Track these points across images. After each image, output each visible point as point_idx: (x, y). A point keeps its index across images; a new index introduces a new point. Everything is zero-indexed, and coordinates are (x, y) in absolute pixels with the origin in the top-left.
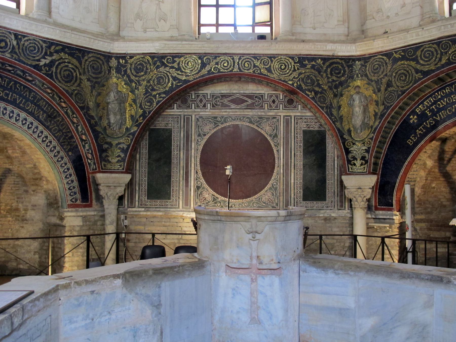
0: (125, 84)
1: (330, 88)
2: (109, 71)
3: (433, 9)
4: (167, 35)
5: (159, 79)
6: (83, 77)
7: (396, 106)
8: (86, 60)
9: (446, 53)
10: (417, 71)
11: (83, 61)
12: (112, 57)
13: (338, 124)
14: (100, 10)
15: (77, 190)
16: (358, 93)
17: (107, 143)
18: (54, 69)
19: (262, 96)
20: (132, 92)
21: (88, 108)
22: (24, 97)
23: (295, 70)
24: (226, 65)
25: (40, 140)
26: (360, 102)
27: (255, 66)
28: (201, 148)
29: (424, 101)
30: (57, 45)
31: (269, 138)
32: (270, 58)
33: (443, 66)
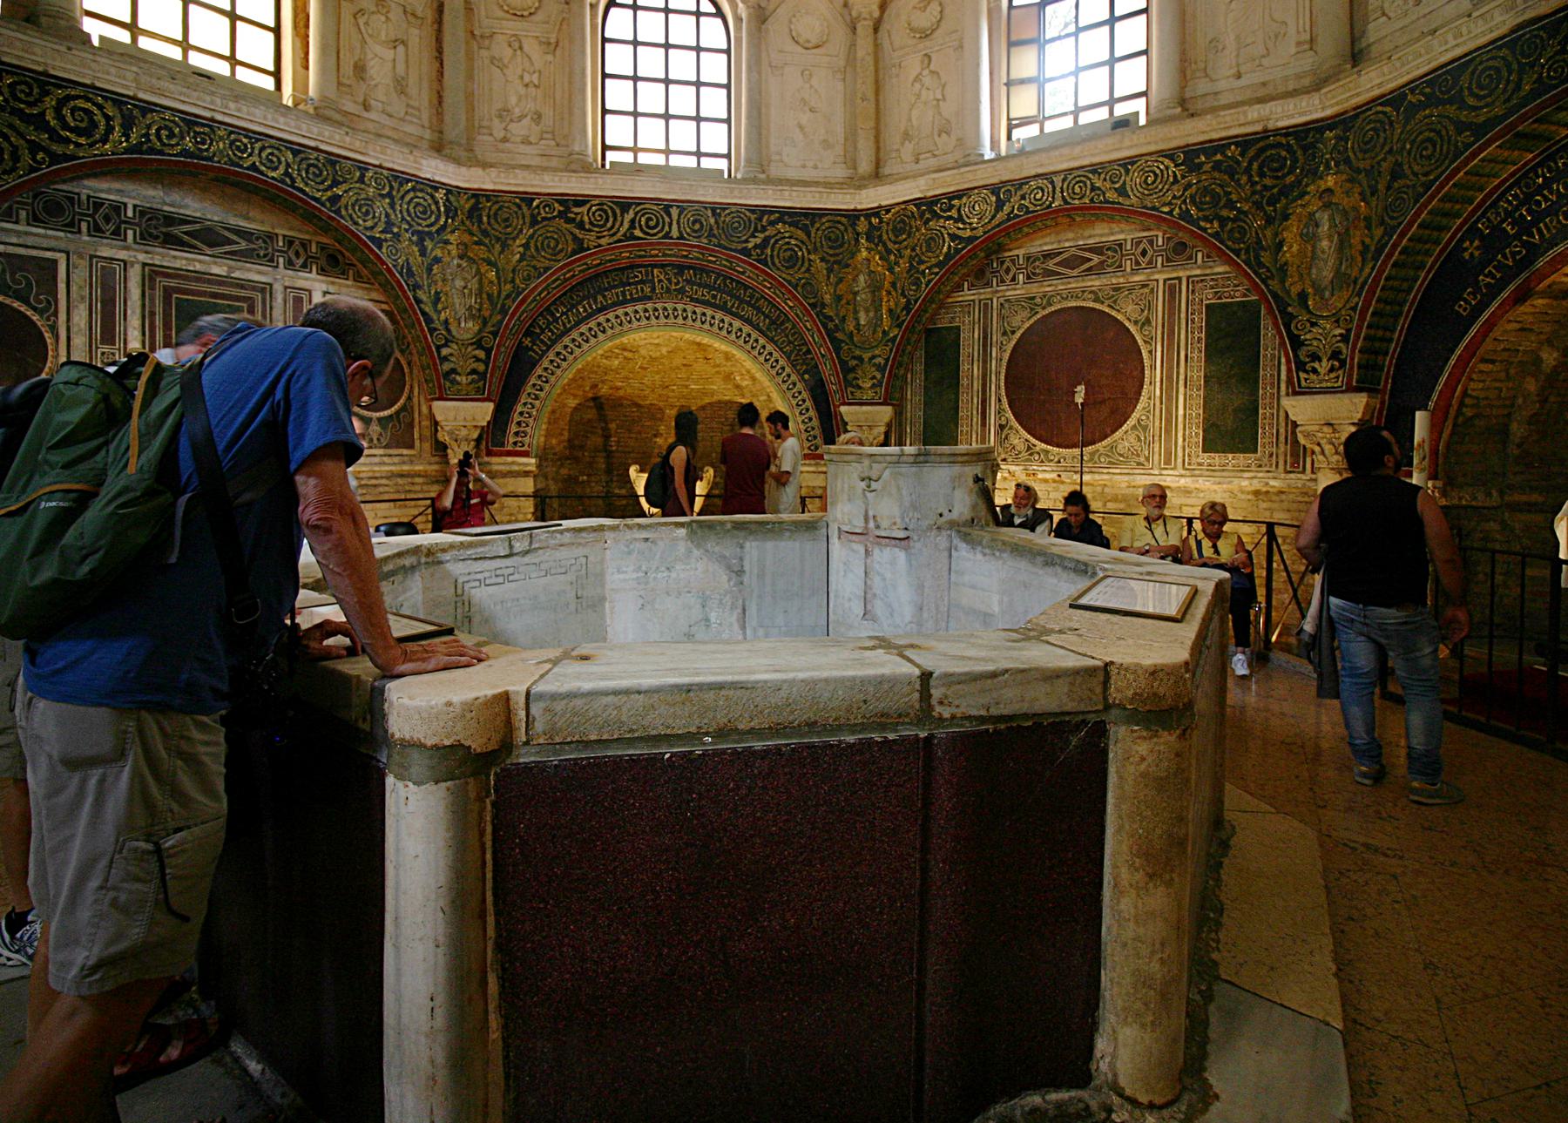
1: (1258, 206)
2: (857, 240)
5: (928, 242)
7: (1411, 224)
11: (813, 231)
12: (858, 217)
13: (1274, 284)
15: (817, 432)
16: (1327, 206)
17: (854, 358)
18: (769, 251)
19: (1120, 245)
20: (891, 270)
21: (823, 305)
22: (738, 298)
25: (762, 359)
26: (1333, 226)
28: (1007, 356)
29: (1499, 199)
30: (772, 213)
31: (1132, 329)
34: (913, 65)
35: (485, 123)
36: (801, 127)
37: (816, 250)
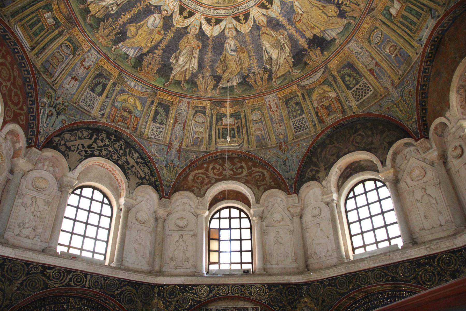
0: (162, 303)
1: (288, 303)
3: (341, 256)
4: (189, 271)
6: (138, 300)
8: (141, 289)
9: (351, 282)
10: (338, 293)
11: (139, 290)
14: (150, 256)
16: (306, 306)
18: (122, 297)
19: (247, 309)
23: (266, 293)
24: (224, 291)
27: (242, 291)
30: (125, 281)
32: (251, 286)
33: (351, 290)
34: (176, 236)
35: (12, 227)
36: (135, 250)
37: (139, 297)
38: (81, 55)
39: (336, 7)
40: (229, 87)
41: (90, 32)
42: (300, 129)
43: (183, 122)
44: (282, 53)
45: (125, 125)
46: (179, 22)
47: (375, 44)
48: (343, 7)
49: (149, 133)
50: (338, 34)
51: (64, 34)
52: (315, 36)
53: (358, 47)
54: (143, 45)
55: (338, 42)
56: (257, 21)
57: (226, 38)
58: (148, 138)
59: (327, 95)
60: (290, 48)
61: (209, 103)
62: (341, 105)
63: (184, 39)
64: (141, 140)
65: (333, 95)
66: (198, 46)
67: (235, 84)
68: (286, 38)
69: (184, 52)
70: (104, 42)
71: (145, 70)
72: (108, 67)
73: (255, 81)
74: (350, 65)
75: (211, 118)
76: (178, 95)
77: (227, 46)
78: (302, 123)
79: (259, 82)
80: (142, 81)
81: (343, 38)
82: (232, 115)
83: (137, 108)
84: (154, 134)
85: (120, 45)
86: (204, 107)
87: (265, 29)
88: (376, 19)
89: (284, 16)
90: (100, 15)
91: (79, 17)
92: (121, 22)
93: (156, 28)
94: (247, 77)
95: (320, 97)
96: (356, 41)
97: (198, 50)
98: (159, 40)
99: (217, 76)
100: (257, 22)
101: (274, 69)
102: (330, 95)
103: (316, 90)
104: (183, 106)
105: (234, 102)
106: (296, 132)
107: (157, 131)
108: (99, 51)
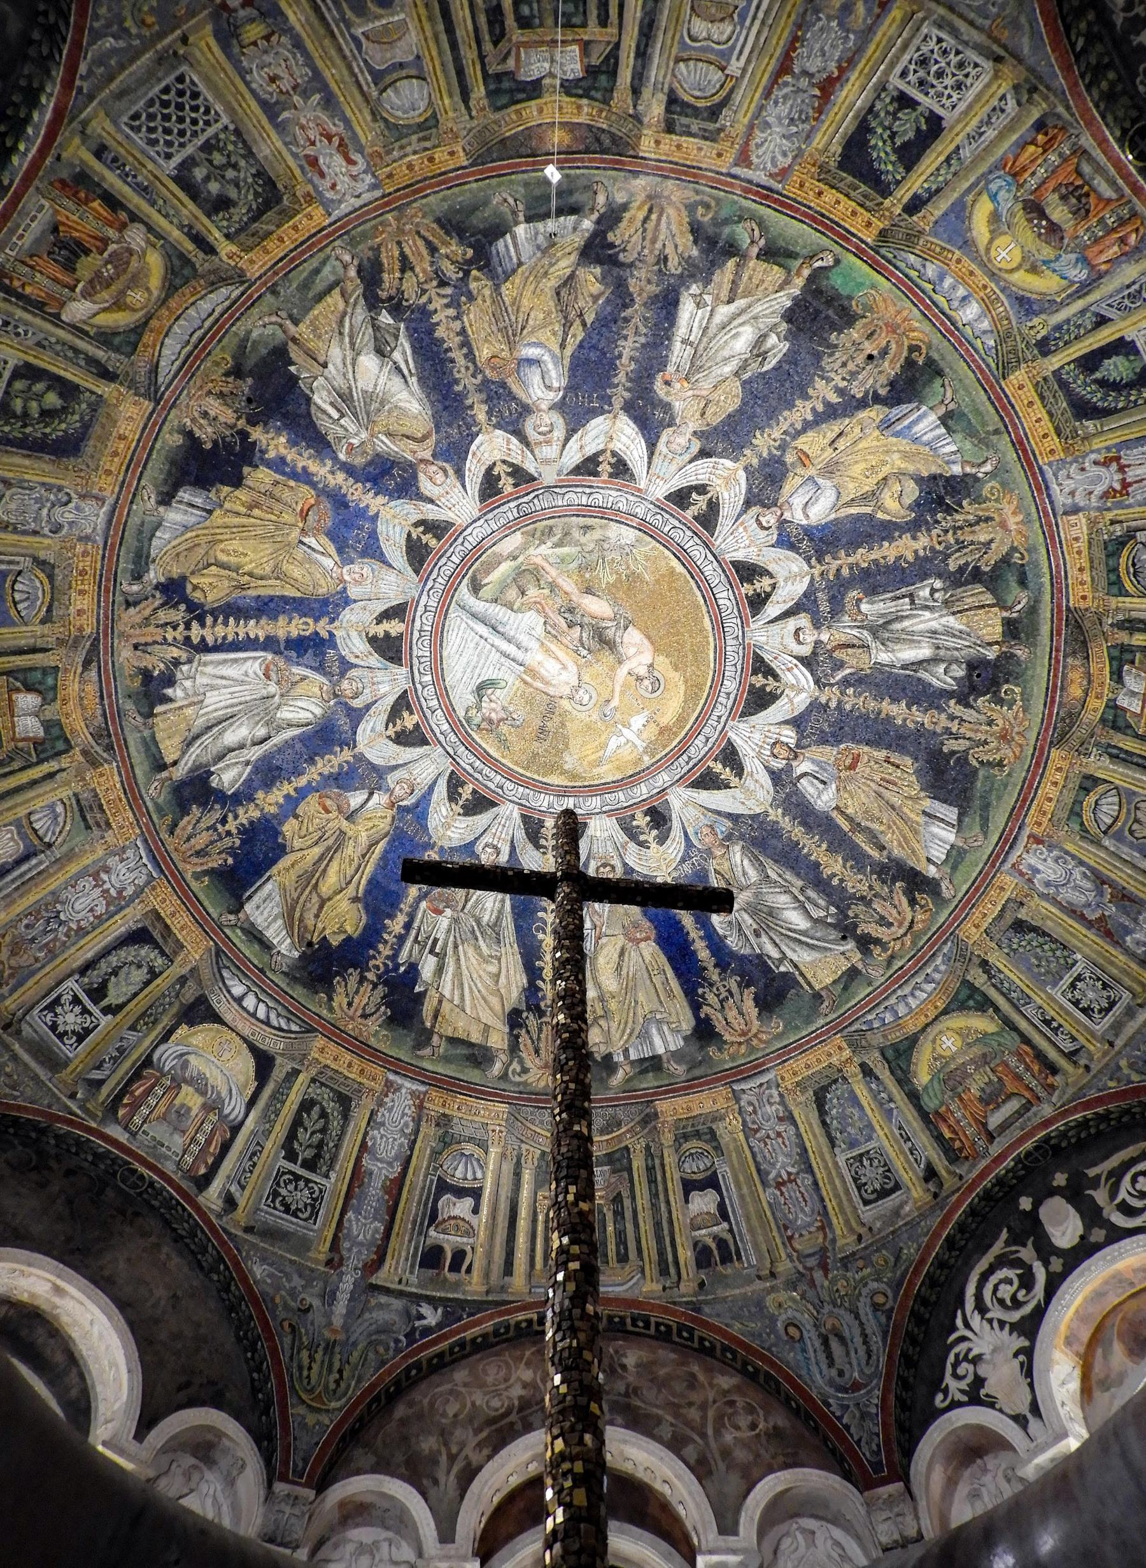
38: (1110, 515)
39: (202, 605)
40: (546, 216)
41: (1036, 564)
42: (165, 104)
43: (788, 78)
44: (339, 382)
45: (1086, 169)
46: (727, 480)
47: (20, 573)
48: (178, 614)
49: (985, 78)
50: (159, 525)
51: (1121, 617)
52: (237, 481)
53: (71, 524)
54: (873, 439)
55: (149, 498)
56: (452, 478)
57: (559, 407)
58: (998, 59)
59: (105, 295)
60: (313, 409)
61: (646, 146)
62: (20, 296)
63: (715, 416)
64: (1042, 68)
65: (78, 310)
66: (667, 383)
67: (521, 230)
68: (340, 439)
69: (728, 369)
70: (1008, 509)
71: (900, 345)
72: (1035, 420)
73: (433, 250)
74: (66, 448)
75: (639, 78)
76: (782, 204)
77: (558, 377)
78: (167, 131)
79: (414, 247)
80: (927, 307)
81: (135, 520)
82: (534, 89)
83: (995, 217)
84: (961, 65)
85: (957, 470)
86: (670, 128)
87: (421, 455)
88: (61, 642)
89: (362, 513)
90: (977, 594)
91: (1045, 629)
92: (922, 542)
93: (811, 478)
94: (469, 262)
95: (124, 278)
96: (86, 539)
97: (671, 369)
98: (810, 434)
99: (599, 261)
100: (451, 472)
101: (361, 313)
102: (88, 304)
103: (156, 293)
104: (772, 148)
105: (523, 150)
106: (181, 79)
107: (940, 74)
108: (1039, 490)
